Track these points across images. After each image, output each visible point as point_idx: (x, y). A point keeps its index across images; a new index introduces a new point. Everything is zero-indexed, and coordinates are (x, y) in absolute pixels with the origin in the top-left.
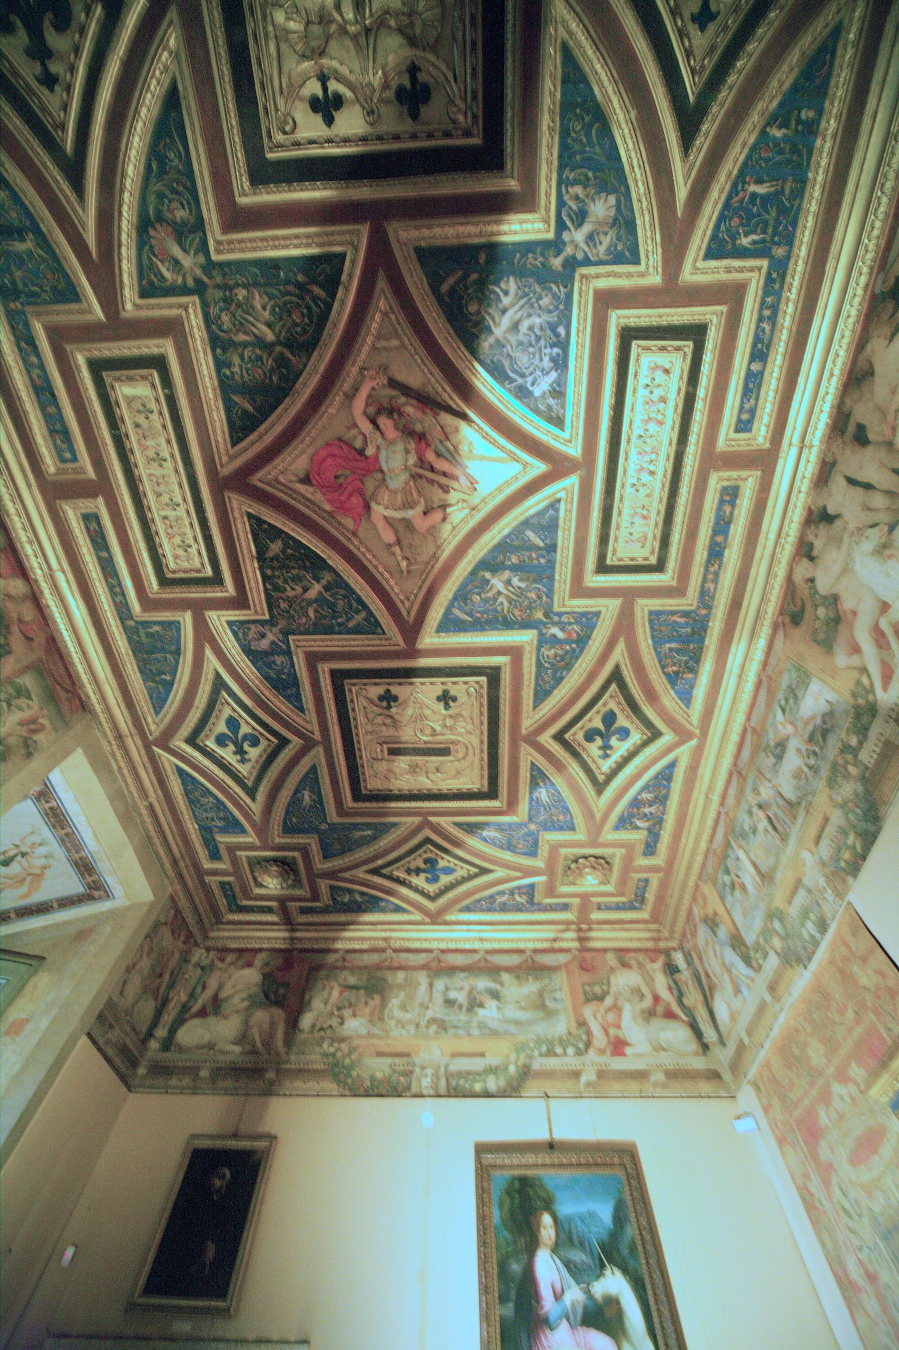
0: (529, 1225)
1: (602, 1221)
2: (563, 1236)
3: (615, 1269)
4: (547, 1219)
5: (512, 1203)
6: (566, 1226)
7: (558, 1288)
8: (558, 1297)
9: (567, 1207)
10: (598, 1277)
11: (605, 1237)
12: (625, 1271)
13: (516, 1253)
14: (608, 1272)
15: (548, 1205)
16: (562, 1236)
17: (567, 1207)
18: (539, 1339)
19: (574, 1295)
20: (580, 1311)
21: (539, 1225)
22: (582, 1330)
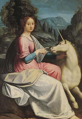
0: (19, 24)
1: (64, 21)
2: (39, 28)
3: (68, 42)
4: (31, 20)
5: (9, 13)
6: (42, 24)
7: (33, 48)
8: (32, 51)
9: (43, 15)
10: (57, 45)
11: (65, 28)
12: (73, 42)
13: (9, 35)
14: (63, 43)
15: (32, 13)
16: (39, 28)
17: (43, 15)
18: (19, 66)
19: (41, 50)
20: (43, 56)
21: (25, 23)
22: (42, 64)
